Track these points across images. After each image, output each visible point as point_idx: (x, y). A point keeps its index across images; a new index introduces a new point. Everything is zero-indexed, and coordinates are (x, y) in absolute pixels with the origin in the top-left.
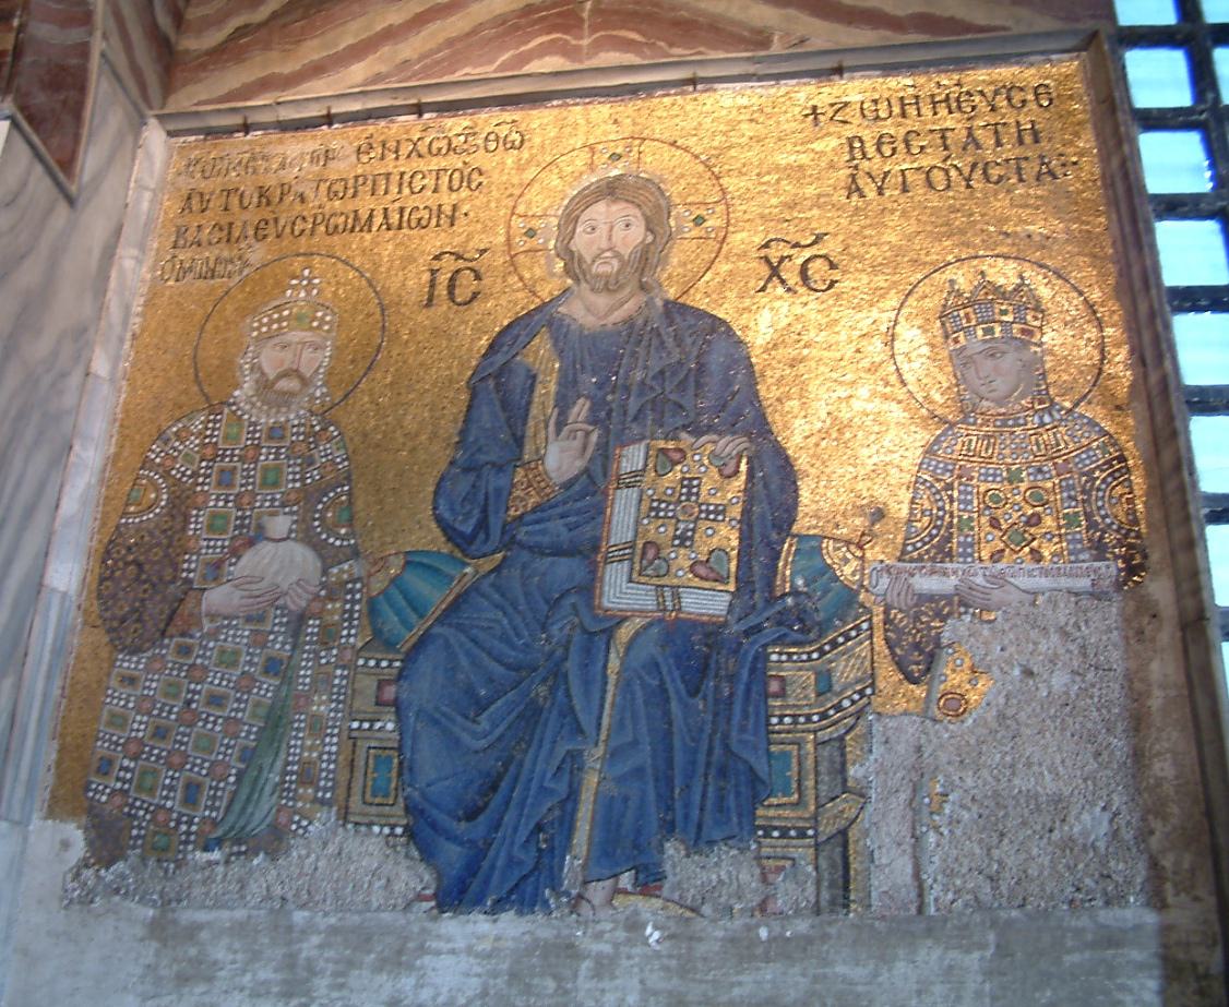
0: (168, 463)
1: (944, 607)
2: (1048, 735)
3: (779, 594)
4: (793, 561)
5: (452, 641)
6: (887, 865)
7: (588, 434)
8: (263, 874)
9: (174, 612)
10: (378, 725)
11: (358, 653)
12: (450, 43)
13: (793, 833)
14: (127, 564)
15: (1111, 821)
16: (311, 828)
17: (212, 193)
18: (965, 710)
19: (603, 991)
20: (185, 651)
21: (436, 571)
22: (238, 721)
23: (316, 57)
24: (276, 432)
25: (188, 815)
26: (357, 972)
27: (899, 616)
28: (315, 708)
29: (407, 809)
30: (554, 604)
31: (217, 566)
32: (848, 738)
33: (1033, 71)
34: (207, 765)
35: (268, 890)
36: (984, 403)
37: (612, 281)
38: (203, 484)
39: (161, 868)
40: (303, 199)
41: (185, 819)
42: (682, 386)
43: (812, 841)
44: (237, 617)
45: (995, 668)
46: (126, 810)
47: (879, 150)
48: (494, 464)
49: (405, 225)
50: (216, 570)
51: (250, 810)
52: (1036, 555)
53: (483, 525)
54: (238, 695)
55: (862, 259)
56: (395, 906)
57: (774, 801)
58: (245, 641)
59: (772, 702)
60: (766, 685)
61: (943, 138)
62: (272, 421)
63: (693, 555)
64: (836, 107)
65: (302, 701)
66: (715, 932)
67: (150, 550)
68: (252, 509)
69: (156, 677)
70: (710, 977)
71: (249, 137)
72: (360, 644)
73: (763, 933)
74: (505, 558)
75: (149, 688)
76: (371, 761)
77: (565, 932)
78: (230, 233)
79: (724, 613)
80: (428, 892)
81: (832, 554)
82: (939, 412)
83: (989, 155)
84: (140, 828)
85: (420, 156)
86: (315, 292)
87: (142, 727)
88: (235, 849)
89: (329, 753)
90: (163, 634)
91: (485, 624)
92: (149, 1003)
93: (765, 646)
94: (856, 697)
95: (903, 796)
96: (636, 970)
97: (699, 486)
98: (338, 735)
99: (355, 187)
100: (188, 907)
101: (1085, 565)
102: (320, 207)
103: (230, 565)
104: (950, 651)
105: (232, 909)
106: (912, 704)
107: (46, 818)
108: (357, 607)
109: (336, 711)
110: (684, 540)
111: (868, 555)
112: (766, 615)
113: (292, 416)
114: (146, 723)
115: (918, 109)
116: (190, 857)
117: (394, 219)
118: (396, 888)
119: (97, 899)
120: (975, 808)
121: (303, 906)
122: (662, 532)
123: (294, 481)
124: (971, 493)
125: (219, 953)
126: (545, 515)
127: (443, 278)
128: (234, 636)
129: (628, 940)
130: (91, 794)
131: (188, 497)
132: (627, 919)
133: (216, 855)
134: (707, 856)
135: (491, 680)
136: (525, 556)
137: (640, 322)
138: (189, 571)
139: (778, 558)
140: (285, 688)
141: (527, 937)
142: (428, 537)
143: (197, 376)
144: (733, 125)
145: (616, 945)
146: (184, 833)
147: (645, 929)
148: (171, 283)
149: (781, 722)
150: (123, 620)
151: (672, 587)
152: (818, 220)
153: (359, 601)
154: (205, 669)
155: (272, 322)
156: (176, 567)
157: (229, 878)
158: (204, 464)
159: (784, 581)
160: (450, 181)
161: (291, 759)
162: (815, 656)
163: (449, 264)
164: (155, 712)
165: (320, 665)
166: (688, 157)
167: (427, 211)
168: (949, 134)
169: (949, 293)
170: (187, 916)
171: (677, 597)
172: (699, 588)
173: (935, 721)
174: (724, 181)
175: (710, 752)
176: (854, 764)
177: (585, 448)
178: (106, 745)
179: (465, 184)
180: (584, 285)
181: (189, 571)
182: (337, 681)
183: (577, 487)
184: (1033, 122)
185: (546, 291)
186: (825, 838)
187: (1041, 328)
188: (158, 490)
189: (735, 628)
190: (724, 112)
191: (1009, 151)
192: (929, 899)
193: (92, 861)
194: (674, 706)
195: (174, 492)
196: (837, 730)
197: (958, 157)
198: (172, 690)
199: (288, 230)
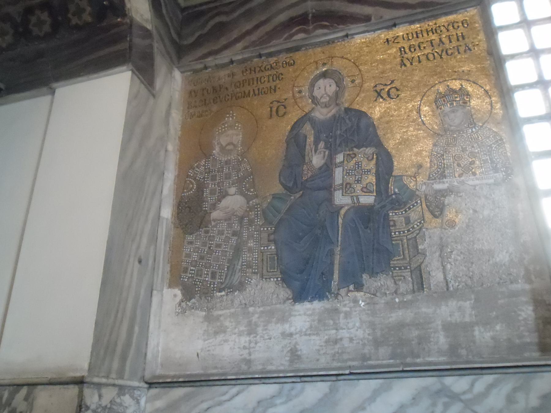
0: (195, 175)
1: (444, 193)
2: (484, 230)
3: (390, 194)
4: (394, 184)
6: (434, 276)
7: (325, 152)
8: (239, 297)
10: (269, 248)
11: (261, 226)
12: (267, 33)
13: (403, 268)
15: (509, 256)
16: (252, 281)
17: (198, 91)
18: (455, 225)
19: (348, 323)
20: (207, 232)
22: (226, 251)
23: (225, 43)
24: (227, 163)
25: (213, 282)
26: (270, 325)
27: (430, 198)
28: (249, 245)
29: (281, 273)
32: (417, 237)
33: (461, 15)
34: (217, 266)
35: (240, 302)
36: (452, 128)
38: (206, 181)
39: (207, 299)
40: (227, 89)
41: (212, 283)
43: (409, 270)
44: (221, 220)
45: (464, 211)
46: (193, 283)
47: (410, 50)
49: (260, 94)
50: (214, 207)
51: (232, 278)
52: (474, 174)
53: (295, 183)
55: (407, 86)
56: (280, 303)
57: (396, 259)
58: (225, 227)
59: (392, 228)
60: (389, 223)
61: (432, 43)
63: (362, 186)
64: (394, 38)
66: (381, 301)
68: (223, 187)
70: (382, 315)
71: (207, 71)
72: (261, 224)
73: (397, 300)
75: (197, 244)
76: (268, 259)
77: (334, 305)
79: (373, 202)
80: (290, 297)
81: (406, 180)
82: (437, 132)
83: (447, 46)
84: (198, 287)
85: (262, 71)
87: (196, 257)
88: (229, 290)
89: (255, 258)
90: (200, 228)
92: (206, 342)
93: (387, 211)
94: (418, 224)
95: (438, 254)
96: (358, 315)
97: (361, 164)
98: (257, 252)
99: (243, 84)
100: (216, 310)
101: (491, 175)
102: (233, 91)
103: (218, 204)
104: (448, 207)
105: (229, 309)
106: (437, 224)
107: (168, 288)
108: (259, 213)
109: (256, 245)
111: (418, 179)
112: (387, 201)
114: (197, 256)
115: (422, 35)
116: (215, 295)
117: (257, 92)
118: (280, 297)
119: (187, 312)
120: (462, 256)
121: (252, 306)
122: (351, 180)
123: (235, 176)
124: (450, 157)
125: (227, 323)
127: (274, 109)
128: (222, 226)
129: (354, 306)
130: (182, 279)
132: (353, 300)
133: (223, 293)
134: (376, 278)
137: (338, 116)
138: (205, 207)
139: (389, 184)
140: (239, 240)
141: (322, 308)
142: (278, 189)
144: (361, 48)
145: (351, 308)
146: (213, 287)
147: (359, 302)
149: (395, 234)
150: (186, 225)
151: (356, 196)
152: (390, 75)
153: (259, 211)
154: (214, 236)
155: (222, 128)
157: (228, 300)
158: (206, 174)
159: (391, 190)
160: (273, 78)
161: (243, 261)
163: (276, 105)
164: (200, 252)
165: (250, 231)
166: (347, 61)
167: (267, 89)
168: (433, 41)
169: (437, 94)
170: (216, 313)
171: (358, 199)
172: (363, 195)
173: (445, 229)
174: (359, 67)
175: (374, 245)
176: (420, 245)
178: (185, 263)
179: (278, 79)
180: (319, 106)
181: (205, 207)
182: (255, 236)
183: (323, 169)
184: (462, 33)
185: (307, 111)
186: (413, 269)
187: (469, 101)
188: (193, 184)
189: (377, 206)
190: (358, 45)
191: (454, 44)
192: (450, 285)
193: (184, 300)
194: (360, 232)
196: (413, 235)
197: (436, 49)
198: (204, 244)
199: (224, 99)
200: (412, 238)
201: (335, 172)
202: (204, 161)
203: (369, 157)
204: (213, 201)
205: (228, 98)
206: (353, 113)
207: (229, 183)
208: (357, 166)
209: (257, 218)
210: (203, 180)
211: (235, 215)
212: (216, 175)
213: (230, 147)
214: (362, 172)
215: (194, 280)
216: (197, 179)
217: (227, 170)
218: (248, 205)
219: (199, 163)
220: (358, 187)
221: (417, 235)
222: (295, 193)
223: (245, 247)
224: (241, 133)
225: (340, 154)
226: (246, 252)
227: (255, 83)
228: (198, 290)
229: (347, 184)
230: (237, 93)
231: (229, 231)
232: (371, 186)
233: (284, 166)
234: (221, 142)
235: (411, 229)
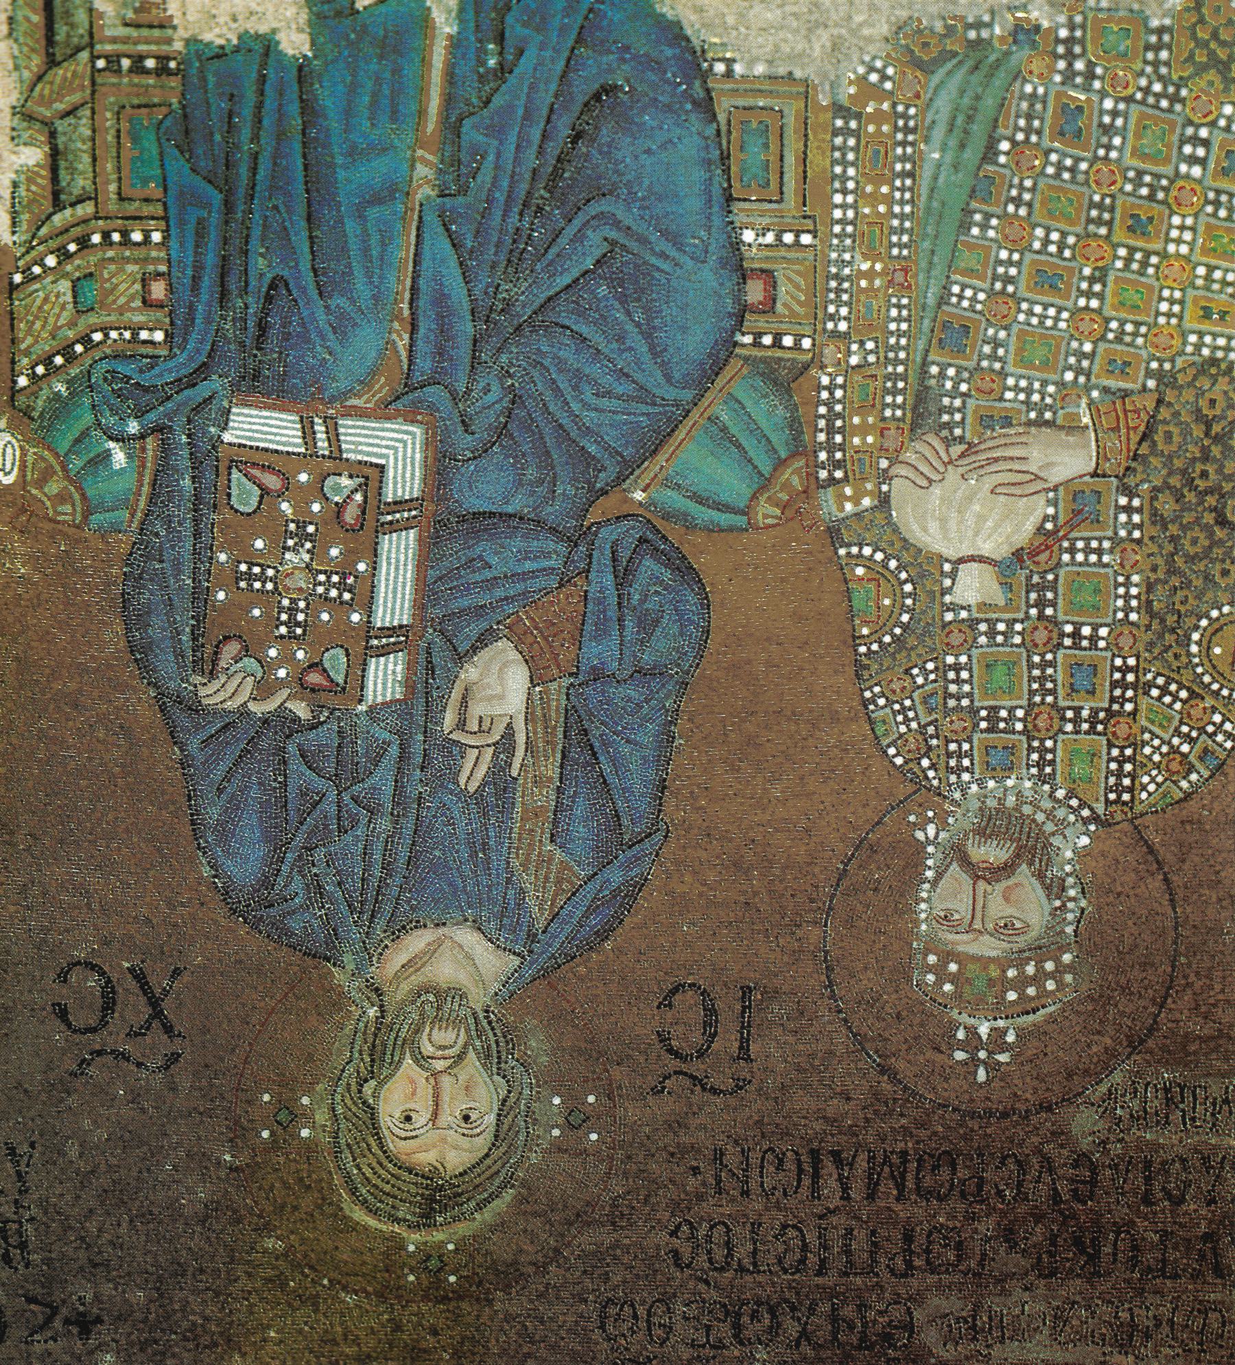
7: (461, 725)
9: (1144, 437)
13: (126, 63)
16: (861, 70)
30: (502, 431)
31: (1077, 517)
44: (1030, 423)
53: (624, 577)
54: (1010, 289)
58: (1011, 381)
62: (1010, 783)
78: (1148, 1180)
79: (234, 410)
86: (961, 1035)
87: (1174, 233)
88: (985, 34)
89: (845, 192)
91: (604, 403)
103: (1055, 518)
113: (974, 787)
114: (1168, 240)
116: (1062, 19)
123: (957, 668)
128: (1029, 391)
131: (1150, 646)
136: (552, 512)
138: (1128, 509)
146: (1075, 57)
155: (1038, 980)
156: (1156, 517)
158: (1129, 707)
161: (908, 182)
162: (97, 337)
164: (1154, 260)
180: (479, 1008)
181: (1128, 509)
182: (844, 311)
183: (473, 630)
189: (215, 383)
194: (305, 265)
200: (73, 205)
202: (1144, 795)
207: (991, 633)
208: (301, 617)
209: (830, 409)
210: (1149, 676)
215: (1178, 107)
216: (1181, 686)
217: (1004, 714)
218: (885, 488)
224: (924, 927)
225: (379, 699)
228: (1157, 48)
231: (989, 357)
234: (1040, 892)
235: (72, 247)
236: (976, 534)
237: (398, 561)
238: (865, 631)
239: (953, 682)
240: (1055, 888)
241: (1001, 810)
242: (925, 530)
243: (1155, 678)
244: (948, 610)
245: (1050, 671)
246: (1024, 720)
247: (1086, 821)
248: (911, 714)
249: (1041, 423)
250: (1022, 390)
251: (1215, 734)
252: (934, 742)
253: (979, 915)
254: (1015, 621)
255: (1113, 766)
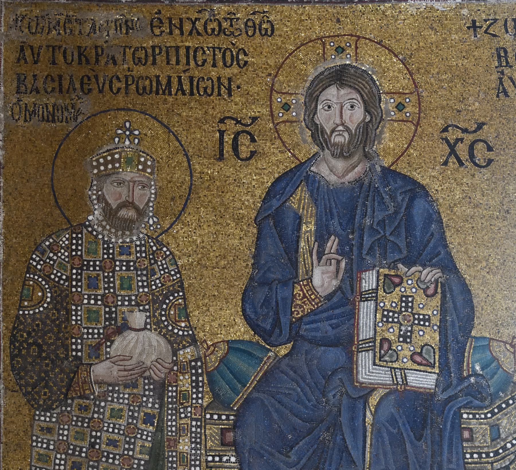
5: (266, 403)
7: (338, 262)
9: (72, 380)
14: (30, 345)
17: (40, 47)
20: (86, 408)
21: (250, 354)
24: (125, 250)
30: (328, 379)
37: (345, 149)
40: (115, 63)
42: (395, 232)
44: (118, 385)
48: (280, 281)
49: (195, 91)
54: (128, 439)
58: (126, 401)
62: (121, 241)
65: (172, 443)
67: (45, 334)
68: (116, 306)
69: (66, 427)
72: (205, 404)
74: (293, 345)
86: (136, 141)
87: (63, 462)
90: (66, 398)
97: (412, 302)
99: (154, 56)
103: (107, 347)
109: (196, 449)
110: (406, 338)
123: (143, 287)
126: (317, 317)
131: (67, 296)
135: (295, 429)
136: (307, 346)
137: (366, 182)
138: (77, 350)
143: (56, 202)
148: (21, 123)
150: (34, 386)
153: (201, 375)
156: (66, 348)
158: (74, 271)
164: (70, 452)
165: (181, 418)
172: (415, 370)
177: (337, 271)
179: (235, 63)
181: (77, 350)
182: (194, 429)
183: (335, 299)
185: (302, 157)
195: (56, 292)
198: (80, 436)
199: (107, 86)
201: (358, 309)
202: (67, 236)
203: (428, 287)
204: (93, 338)
205: (118, 85)
206: (400, 182)
207: (130, 301)
208: (403, 304)
209: (197, 390)
210: (67, 284)
211: (149, 378)
212: (98, 275)
213: (131, 213)
214: (415, 319)
216: (53, 280)
217: (124, 268)
218: (175, 358)
219: (54, 241)
220: (406, 350)
221: (511, 463)
222: (277, 346)
223: (172, 452)
225: (371, 272)
226: (175, 462)
227: (183, 60)
229: (384, 340)
230: (139, 78)
231: (136, 411)
232: (430, 353)
233: (251, 279)
234: (107, 197)
236: (137, 340)
237: (366, 327)
238: (180, 301)
239: (145, 281)
240: (101, 199)
241: (123, 230)
242: (158, 341)
243: (64, 283)
244: (147, 310)
245: (106, 286)
246: (116, 266)
247: (90, 226)
248: (161, 268)
249: (113, 385)
250: (121, 398)
251: (40, 261)
252: (151, 257)
253: (131, 188)
254: (120, 306)
255: (80, 248)
